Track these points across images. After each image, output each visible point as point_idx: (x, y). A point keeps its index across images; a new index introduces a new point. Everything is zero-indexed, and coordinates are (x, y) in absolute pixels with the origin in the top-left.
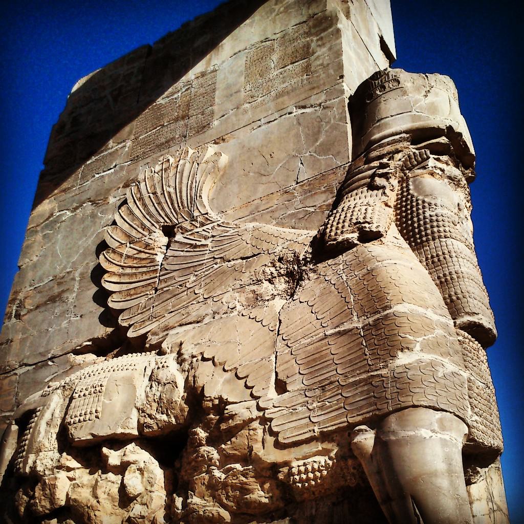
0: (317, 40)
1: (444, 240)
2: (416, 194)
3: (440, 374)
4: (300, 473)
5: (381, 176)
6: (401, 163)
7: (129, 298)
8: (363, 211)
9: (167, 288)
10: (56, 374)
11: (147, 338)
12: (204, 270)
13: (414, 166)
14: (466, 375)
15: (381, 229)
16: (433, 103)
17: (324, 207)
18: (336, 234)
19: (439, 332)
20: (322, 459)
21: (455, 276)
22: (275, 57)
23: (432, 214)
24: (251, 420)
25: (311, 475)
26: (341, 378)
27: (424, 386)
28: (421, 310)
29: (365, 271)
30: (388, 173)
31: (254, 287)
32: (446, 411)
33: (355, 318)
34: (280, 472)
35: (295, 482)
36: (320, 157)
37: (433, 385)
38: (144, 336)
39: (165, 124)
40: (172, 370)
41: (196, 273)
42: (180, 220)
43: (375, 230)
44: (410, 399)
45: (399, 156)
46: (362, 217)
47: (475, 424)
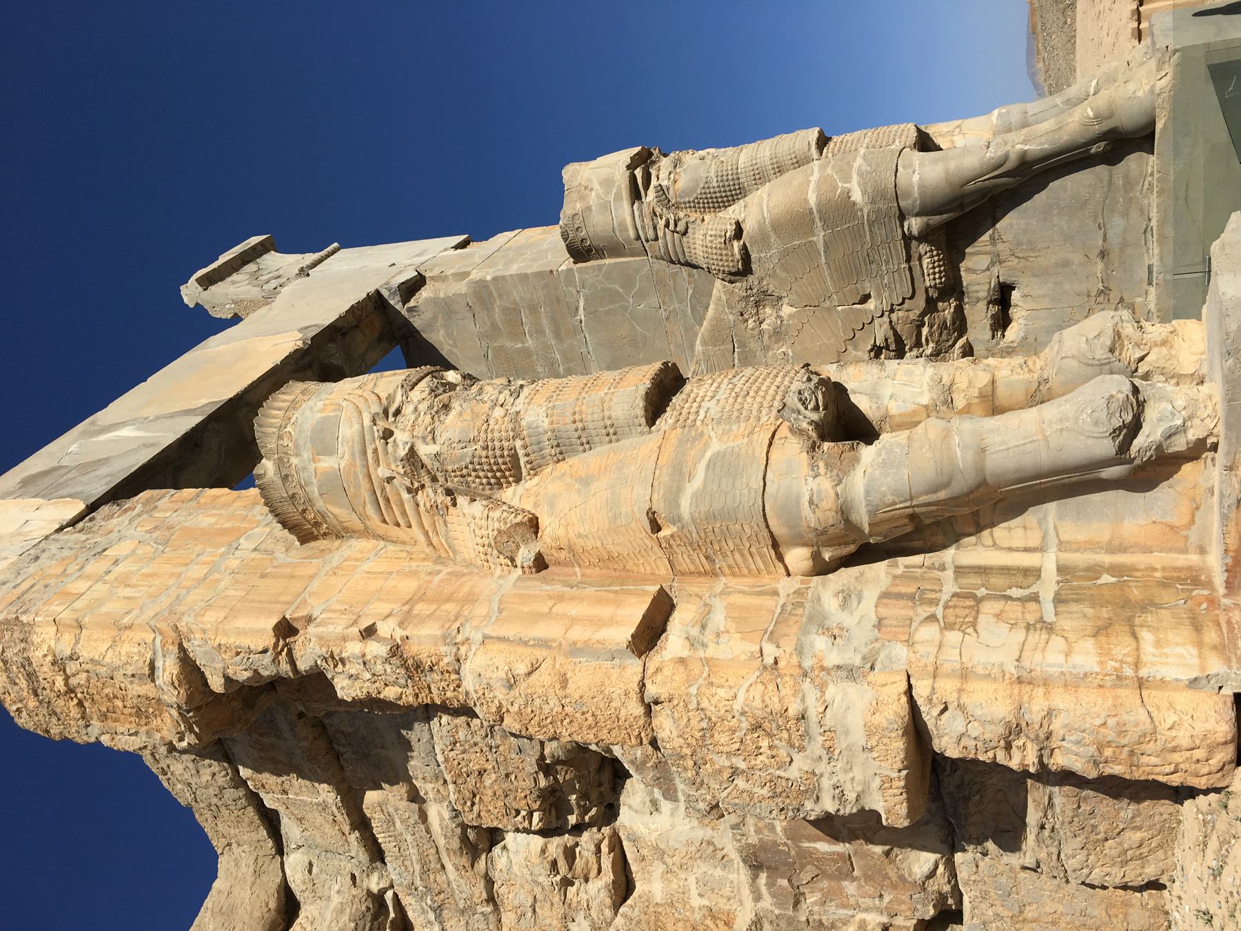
0: (500, 300)
4: (934, 279)
5: (676, 225)
8: (713, 238)
14: (862, 151)
16: (600, 184)
18: (732, 261)
20: (926, 261)
21: (774, 161)
23: (715, 180)
24: (891, 322)
25: (937, 270)
28: (812, 185)
33: (815, 239)
35: (941, 283)
43: (734, 227)
45: (658, 210)
46: (719, 240)
47: (902, 143)
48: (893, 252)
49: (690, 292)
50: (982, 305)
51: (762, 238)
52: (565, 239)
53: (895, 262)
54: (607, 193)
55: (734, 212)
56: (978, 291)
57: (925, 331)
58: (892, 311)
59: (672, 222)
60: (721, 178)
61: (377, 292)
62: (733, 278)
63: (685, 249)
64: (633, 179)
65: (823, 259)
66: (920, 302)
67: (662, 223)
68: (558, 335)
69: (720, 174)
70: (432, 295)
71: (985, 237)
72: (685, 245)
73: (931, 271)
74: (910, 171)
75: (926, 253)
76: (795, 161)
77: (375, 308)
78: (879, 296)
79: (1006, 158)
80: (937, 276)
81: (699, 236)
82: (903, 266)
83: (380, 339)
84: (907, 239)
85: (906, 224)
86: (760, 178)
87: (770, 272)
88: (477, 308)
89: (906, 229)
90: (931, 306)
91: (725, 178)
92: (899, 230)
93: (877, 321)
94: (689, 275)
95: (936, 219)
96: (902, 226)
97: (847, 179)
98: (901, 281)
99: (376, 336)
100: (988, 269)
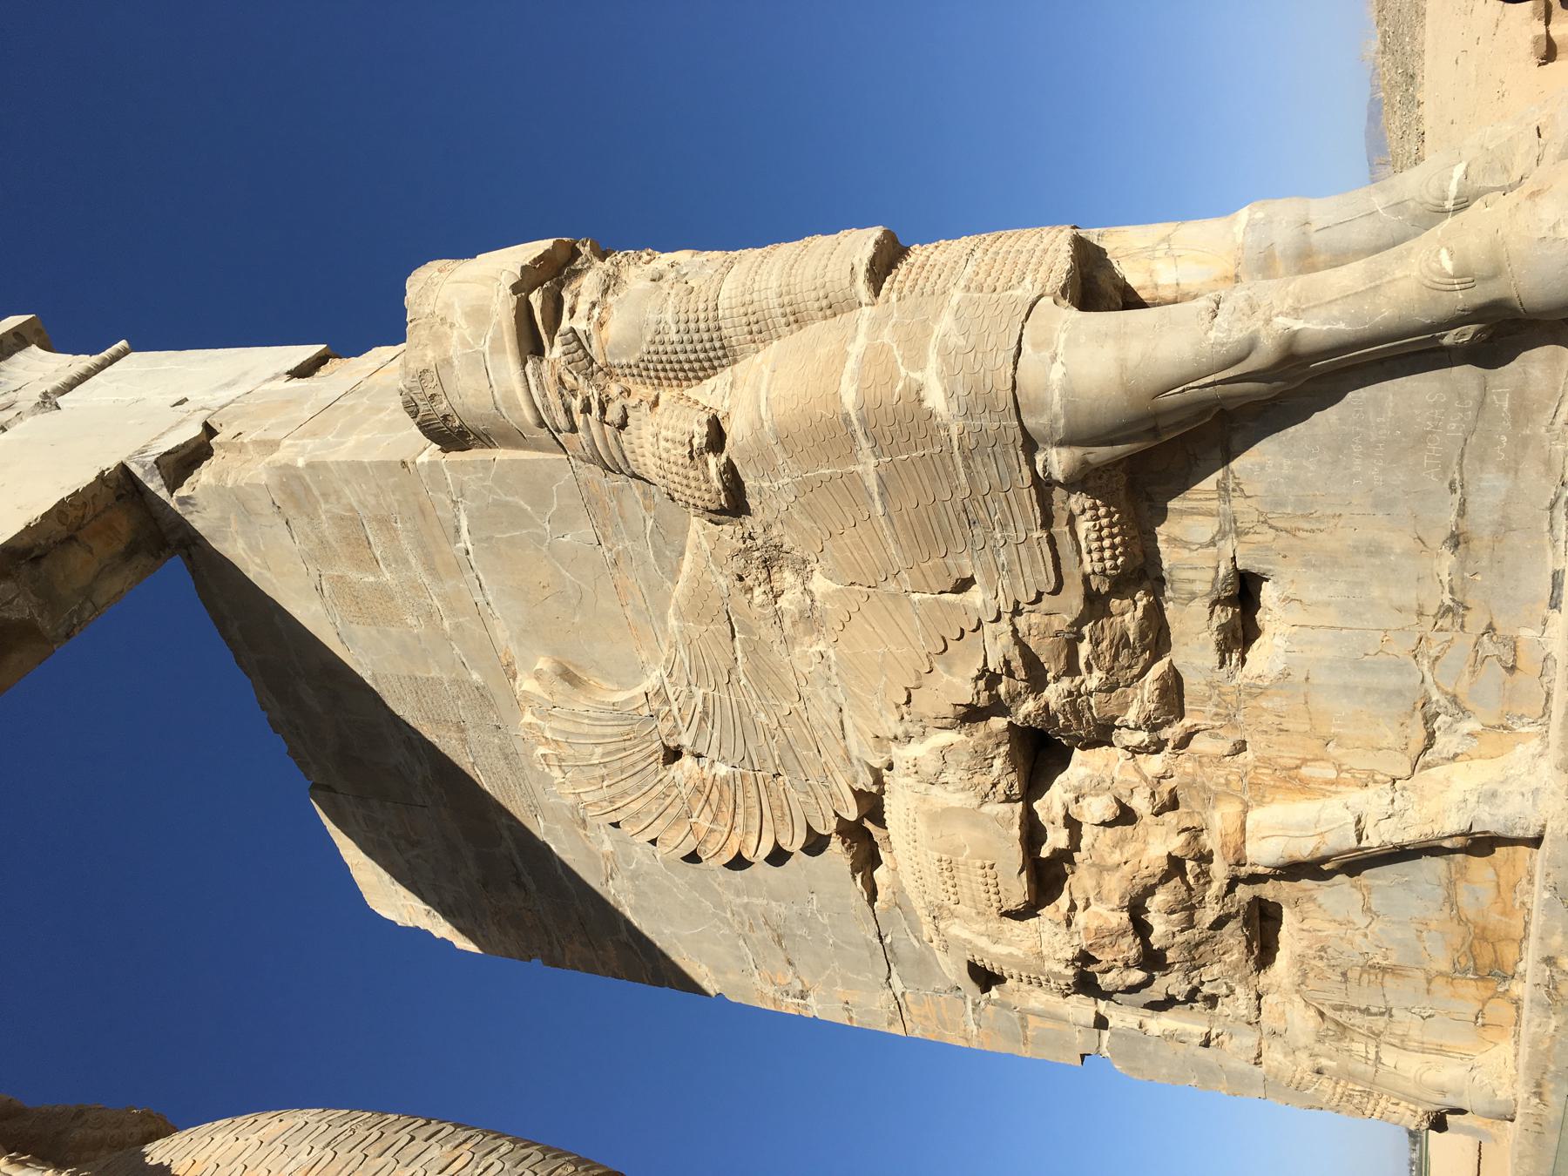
0: (327, 502)
1: (720, 312)
2: (638, 355)
3: (962, 342)
4: (1102, 560)
5: (603, 411)
6: (581, 379)
7: (788, 819)
8: (669, 445)
9: (776, 758)
10: (908, 930)
11: (861, 790)
12: (749, 700)
13: (587, 355)
14: (957, 295)
15: (705, 417)
16: (467, 315)
17: (647, 502)
18: (708, 491)
19: (886, 336)
20: (1084, 526)
21: (786, 299)
22: (353, 575)
23: (674, 329)
24: (1015, 631)
25: (1106, 543)
26: (959, 496)
27: (982, 370)
28: (851, 364)
29: (777, 449)
30: (600, 401)
31: (787, 622)
32: (1021, 335)
34: (1098, 589)
35: (1116, 567)
36: (555, 506)
37: (980, 356)
38: (859, 795)
39: (472, 760)
40: (918, 751)
41: (753, 712)
42: (655, 736)
43: (706, 429)
44: (1001, 395)
45: (568, 378)
46: (680, 450)
47: (1038, 286)
48: (1015, 508)
49: (650, 523)
50: (1200, 607)
51: (763, 458)
52: (414, 415)
53: (1021, 527)
54: (478, 336)
55: (711, 393)
56: (1192, 581)
57: (1084, 649)
58: (1017, 611)
59: (595, 405)
60: (686, 326)
61: (123, 468)
62: (716, 518)
63: (627, 453)
64: (524, 312)
65: (879, 509)
66: (1073, 600)
67: (576, 404)
68: (431, 569)
69: (683, 317)
70: (212, 481)
71: (1209, 483)
72: (625, 446)
73: (1095, 545)
74: (1047, 354)
75: (1083, 512)
76: (824, 303)
77: (118, 498)
78: (990, 583)
79: (1251, 346)
80: (1107, 554)
81: (647, 432)
82: (1036, 535)
83: (130, 553)
84: (1043, 487)
85: (1039, 458)
86: (760, 331)
87: (783, 516)
88: (291, 512)
89: (1039, 468)
90: (1095, 605)
91: (692, 326)
92: (1026, 471)
93: (988, 629)
94: (644, 494)
95: (1101, 453)
96: (1031, 463)
97: (918, 363)
98: (1033, 562)
99: (121, 547)
100: (1213, 543)
